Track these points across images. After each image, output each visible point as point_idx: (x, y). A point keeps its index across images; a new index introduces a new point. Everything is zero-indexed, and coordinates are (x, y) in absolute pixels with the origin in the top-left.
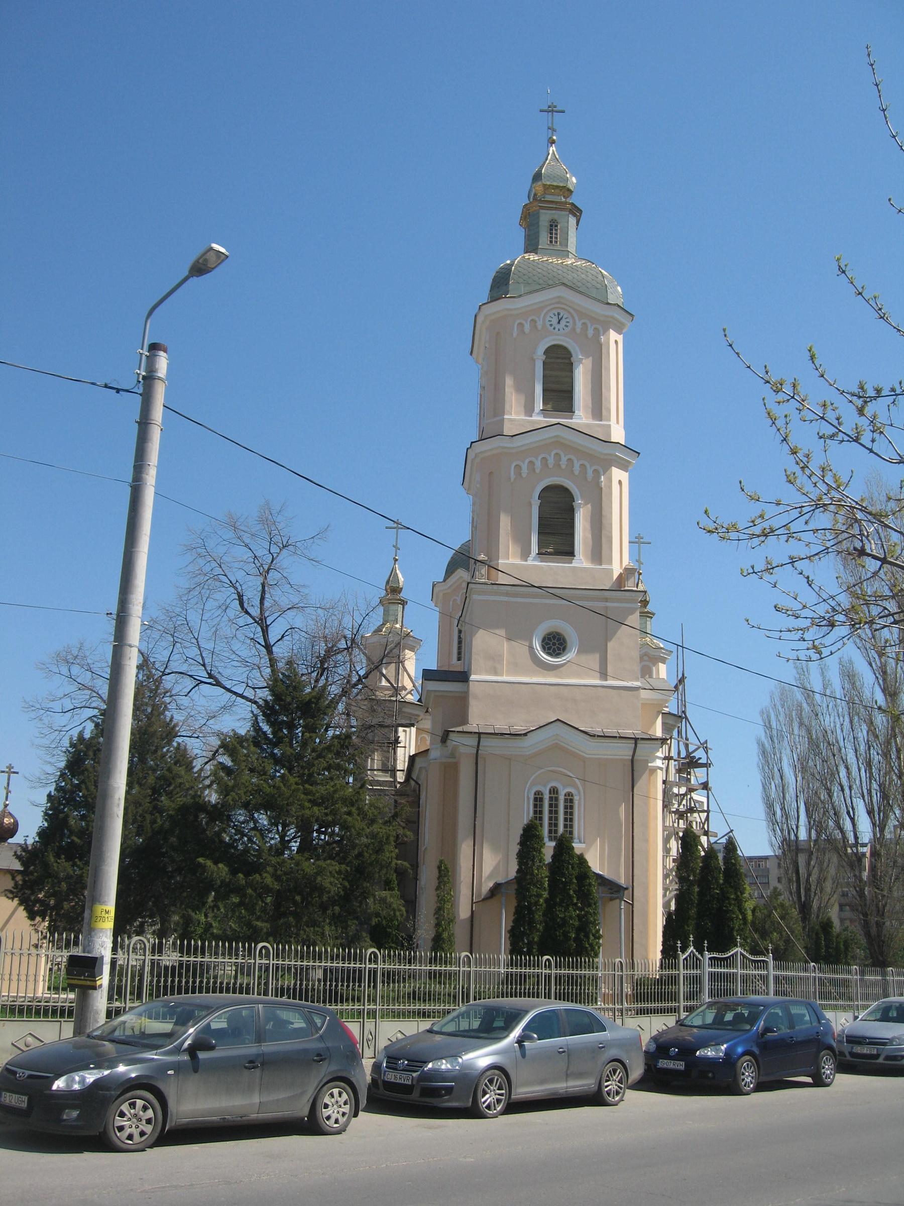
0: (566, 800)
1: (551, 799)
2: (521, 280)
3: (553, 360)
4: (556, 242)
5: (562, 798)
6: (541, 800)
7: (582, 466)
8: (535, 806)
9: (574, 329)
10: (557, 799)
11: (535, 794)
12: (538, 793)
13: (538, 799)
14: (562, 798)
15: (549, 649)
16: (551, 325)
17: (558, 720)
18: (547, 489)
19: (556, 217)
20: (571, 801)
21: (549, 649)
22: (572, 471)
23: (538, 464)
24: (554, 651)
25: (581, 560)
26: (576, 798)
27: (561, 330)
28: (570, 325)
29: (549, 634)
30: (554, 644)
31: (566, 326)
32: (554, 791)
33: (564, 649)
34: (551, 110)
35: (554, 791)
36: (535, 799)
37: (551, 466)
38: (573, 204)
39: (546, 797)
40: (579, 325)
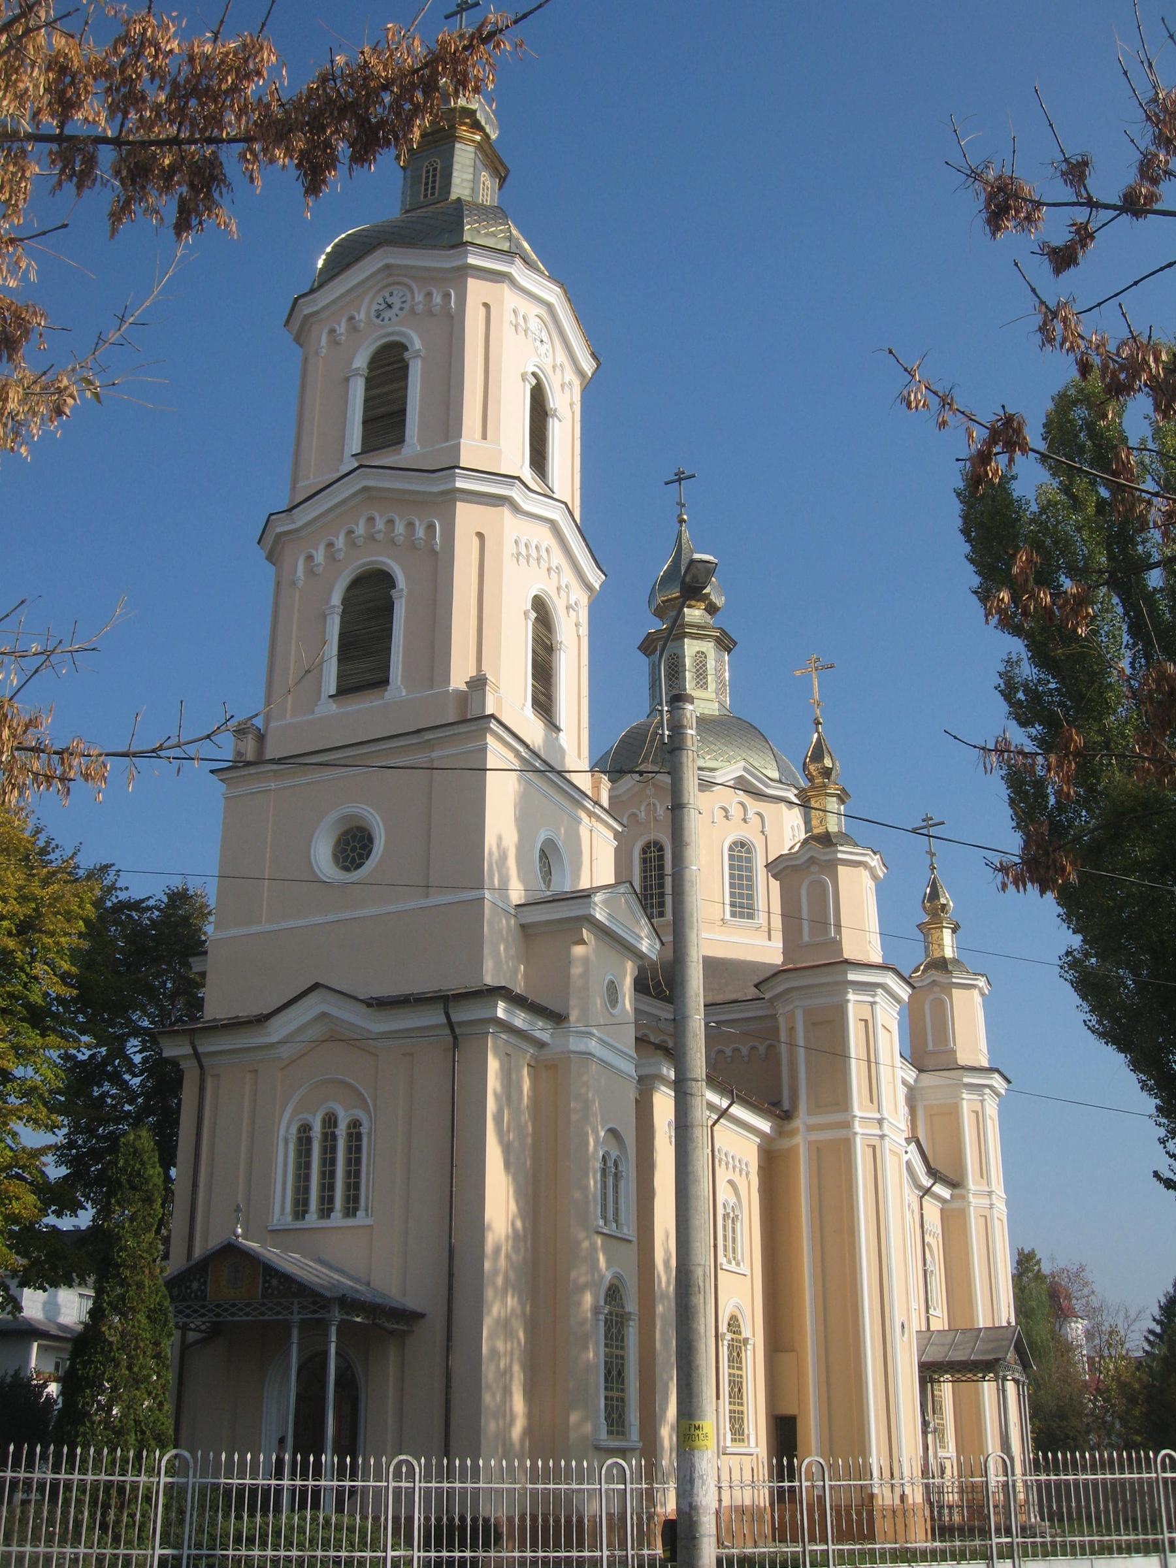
0: (350, 1135)
3: (379, 371)
4: (433, 194)
5: (341, 1131)
6: (309, 1140)
7: (410, 525)
9: (412, 312)
10: (334, 1137)
14: (341, 1131)
17: (316, 986)
20: (359, 1137)
23: (340, 542)
24: (353, 861)
26: (364, 1130)
27: (394, 318)
28: (407, 306)
29: (346, 833)
30: (353, 849)
31: (401, 309)
32: (330, 1121)
35: (330, 1121)
37: (360, 542)
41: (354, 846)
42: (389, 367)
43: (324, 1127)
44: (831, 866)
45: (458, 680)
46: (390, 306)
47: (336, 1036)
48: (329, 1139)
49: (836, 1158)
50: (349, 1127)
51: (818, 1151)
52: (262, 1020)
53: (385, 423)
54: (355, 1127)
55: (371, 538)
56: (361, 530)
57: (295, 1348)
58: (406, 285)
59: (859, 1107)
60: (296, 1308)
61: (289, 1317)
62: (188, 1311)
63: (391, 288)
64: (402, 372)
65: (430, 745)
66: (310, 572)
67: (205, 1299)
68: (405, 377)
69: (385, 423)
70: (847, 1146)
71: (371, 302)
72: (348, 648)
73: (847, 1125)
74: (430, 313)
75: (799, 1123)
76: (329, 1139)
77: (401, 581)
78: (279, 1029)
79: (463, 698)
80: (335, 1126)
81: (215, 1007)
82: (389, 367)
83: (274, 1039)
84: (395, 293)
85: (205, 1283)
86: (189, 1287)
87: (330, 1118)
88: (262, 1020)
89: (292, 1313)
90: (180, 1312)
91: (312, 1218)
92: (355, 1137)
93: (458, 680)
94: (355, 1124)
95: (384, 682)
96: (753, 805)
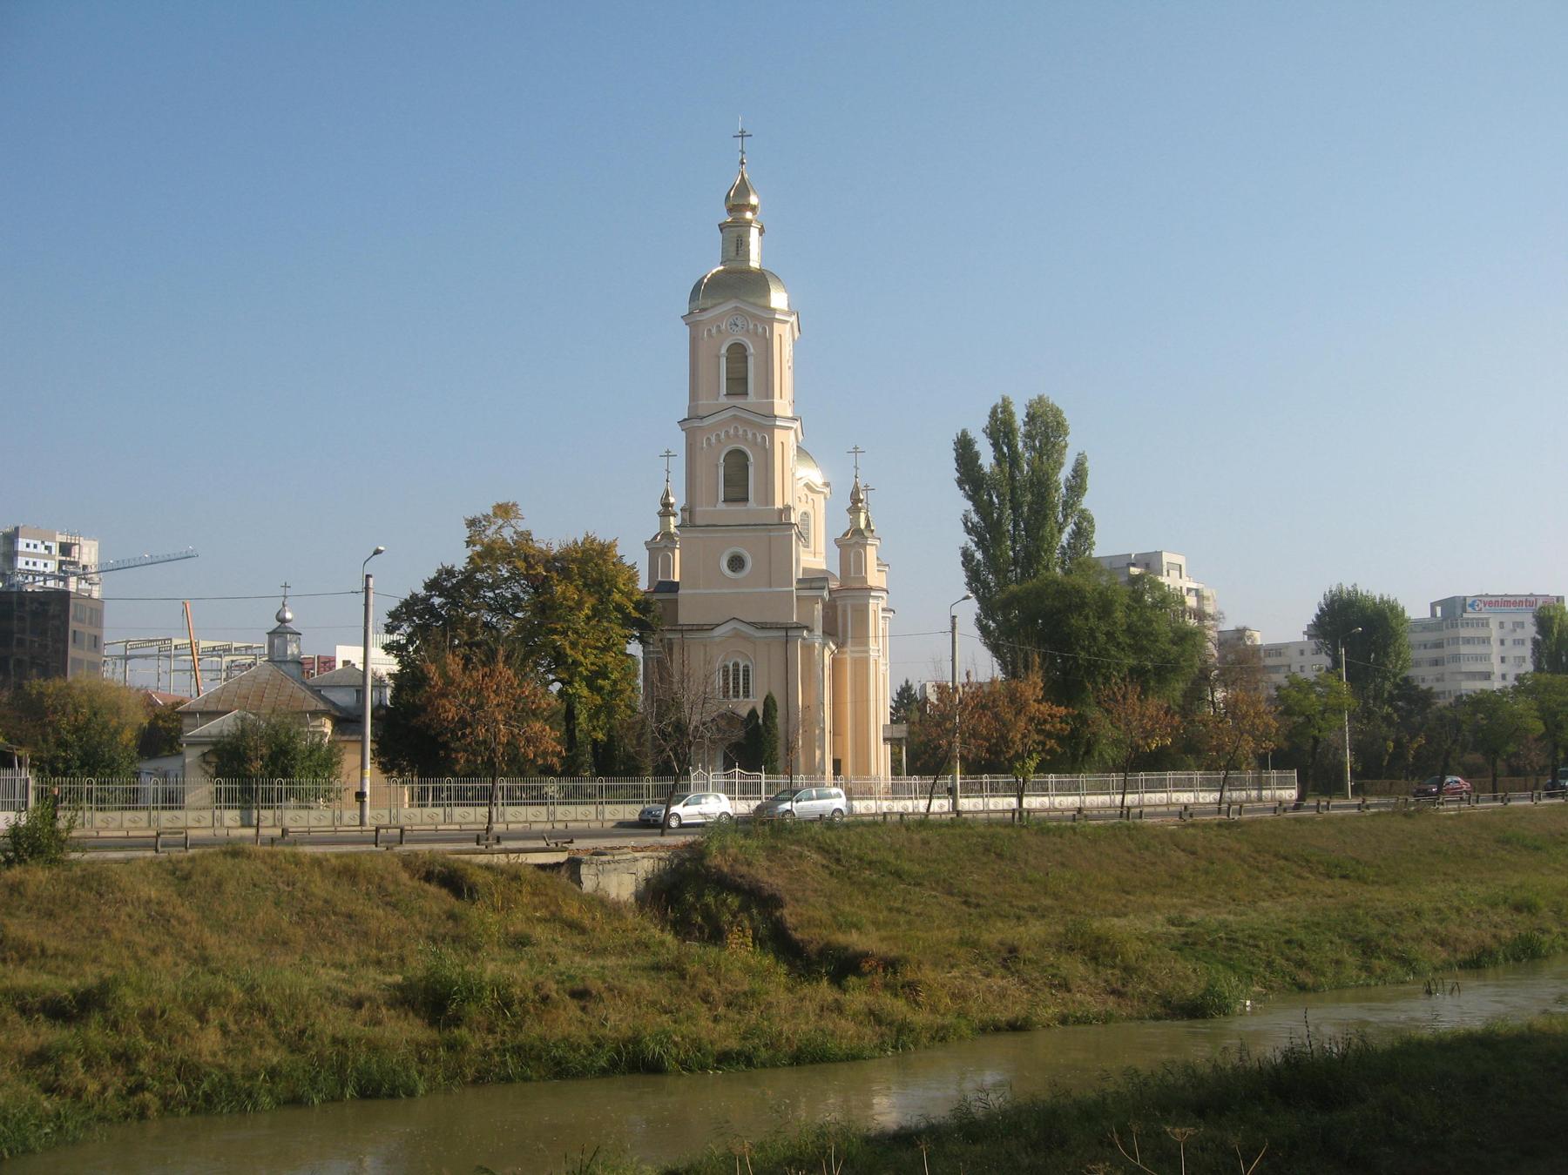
13: (726, 672)
18: (730, 453)
32: (736, 665)
34: (743, 135)
35: (736, 665)
41: (736, 563)
42: (738, 354)
44: (864, 546)
45: (778, 505)
47: (737, 635)
48: (736, 671)
49: (862, 665)
51: (855, 661)
53: (738, 385)
55: (736, 436)
59: (872, 646)
66: (709, 444)
69: (738, 385)
70: (866, 661)
73: (867, 652)
74: (756, 333)
75: (849, 648)
76: (736, 671)
78: (718, 632)
79: (781, 511)
81: (684, 618)
82: (738, 354)
92: (746, 671)
93: (778, 505)
95: (746, 499)
96: (811, 495)
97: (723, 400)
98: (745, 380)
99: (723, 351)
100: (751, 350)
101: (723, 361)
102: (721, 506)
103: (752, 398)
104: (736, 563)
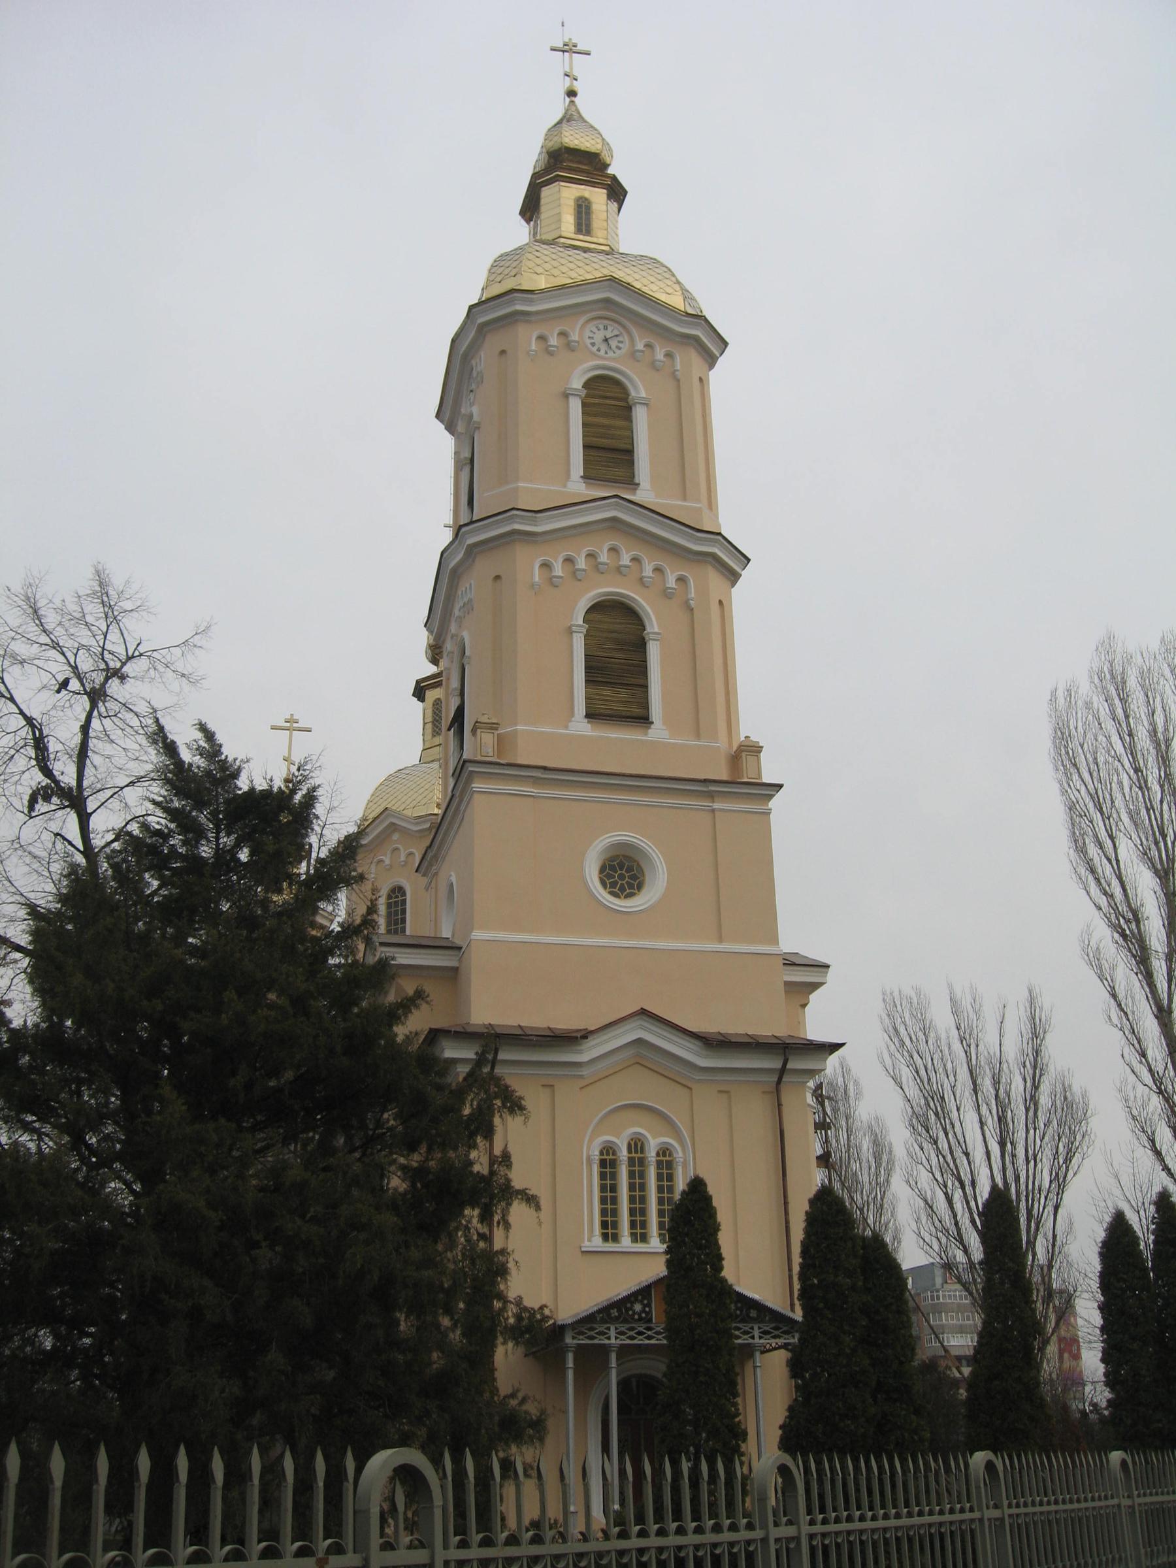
0: (659, 1164)
1: (631, 1161)
2: (539, 270)
3: (597, 401)
5: (651, 1155)
6: (614, 1164)
8: (603, 1176)
10: (642, 1162)
11: (601, 1153)
12: (608, 1150)
13: (608, 1164)
15: (613, 885)
16: (593, 344)
17: (643, 1012)
18: (597, 609)
19: (587, 195)
20: (670, 1165)
21: (613, 885)
22: (641, 579)
24: (622, 889)
25: (658, 731)
28: (626, 347)
29: (612, 859)
30: (622, 877)
31: (619, 348)
32: (637, 1145)
33: (640, 887)
35: (637, 1145)
36: (603, 1163)
38: (614, 178)
39: (623, 1154)
40: (640, 346)
41: (623, 872)
43: (629, 1151)
46: (606, 340)
50: (658, 1154)
52: (586, 1035)
54: (664, 1155)
56: (604, 557)
57: (614, 1373)
58: (624, 327)
60: (756, 1333)
61: (751, 1341)
62: (632, 1333)
63: (606, 322)
64: (625, 410)
65: (711, 796)
67: (650, 1320)
68: (629, 418)
69: (610, 455)
71: (583, 326)
72: (596, 672)
77: (653, 625)
80: (642, 1152)
82: (607, 402)
83: (584, 1058)
84: (610, 328)
85: (649, 1305)
86: (631, 1309)
87: (636, 1144)
88: (586, 1035)
89: (753, 1337)
90: (622, 1333)
91: (626, 1242)
94: (664, 1151)
95: (643, 719)
97: (577, 488)
98: (630, 452)
99: (577, 383)
100: (639, 390)
101: (576, 406)
102: (581, 726)
103: (645, 494)
104: (623, 872)
